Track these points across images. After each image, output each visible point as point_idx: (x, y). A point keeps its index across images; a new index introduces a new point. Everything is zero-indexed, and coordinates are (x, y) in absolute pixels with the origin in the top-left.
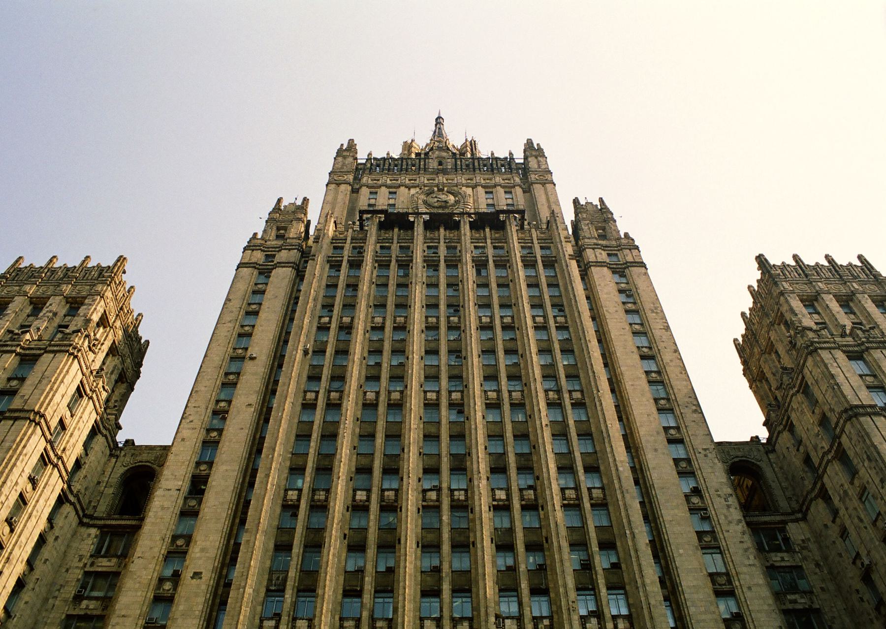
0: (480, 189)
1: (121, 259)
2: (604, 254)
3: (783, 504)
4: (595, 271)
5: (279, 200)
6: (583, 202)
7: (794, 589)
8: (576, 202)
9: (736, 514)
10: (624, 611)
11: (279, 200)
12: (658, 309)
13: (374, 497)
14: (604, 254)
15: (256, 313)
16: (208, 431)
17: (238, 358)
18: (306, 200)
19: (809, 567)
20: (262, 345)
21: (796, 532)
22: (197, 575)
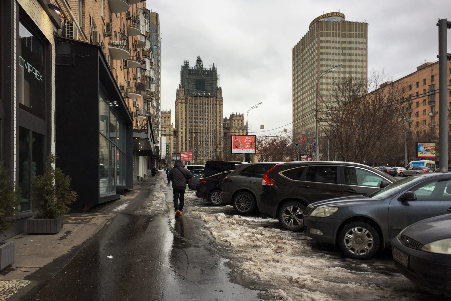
12: (222, 113)
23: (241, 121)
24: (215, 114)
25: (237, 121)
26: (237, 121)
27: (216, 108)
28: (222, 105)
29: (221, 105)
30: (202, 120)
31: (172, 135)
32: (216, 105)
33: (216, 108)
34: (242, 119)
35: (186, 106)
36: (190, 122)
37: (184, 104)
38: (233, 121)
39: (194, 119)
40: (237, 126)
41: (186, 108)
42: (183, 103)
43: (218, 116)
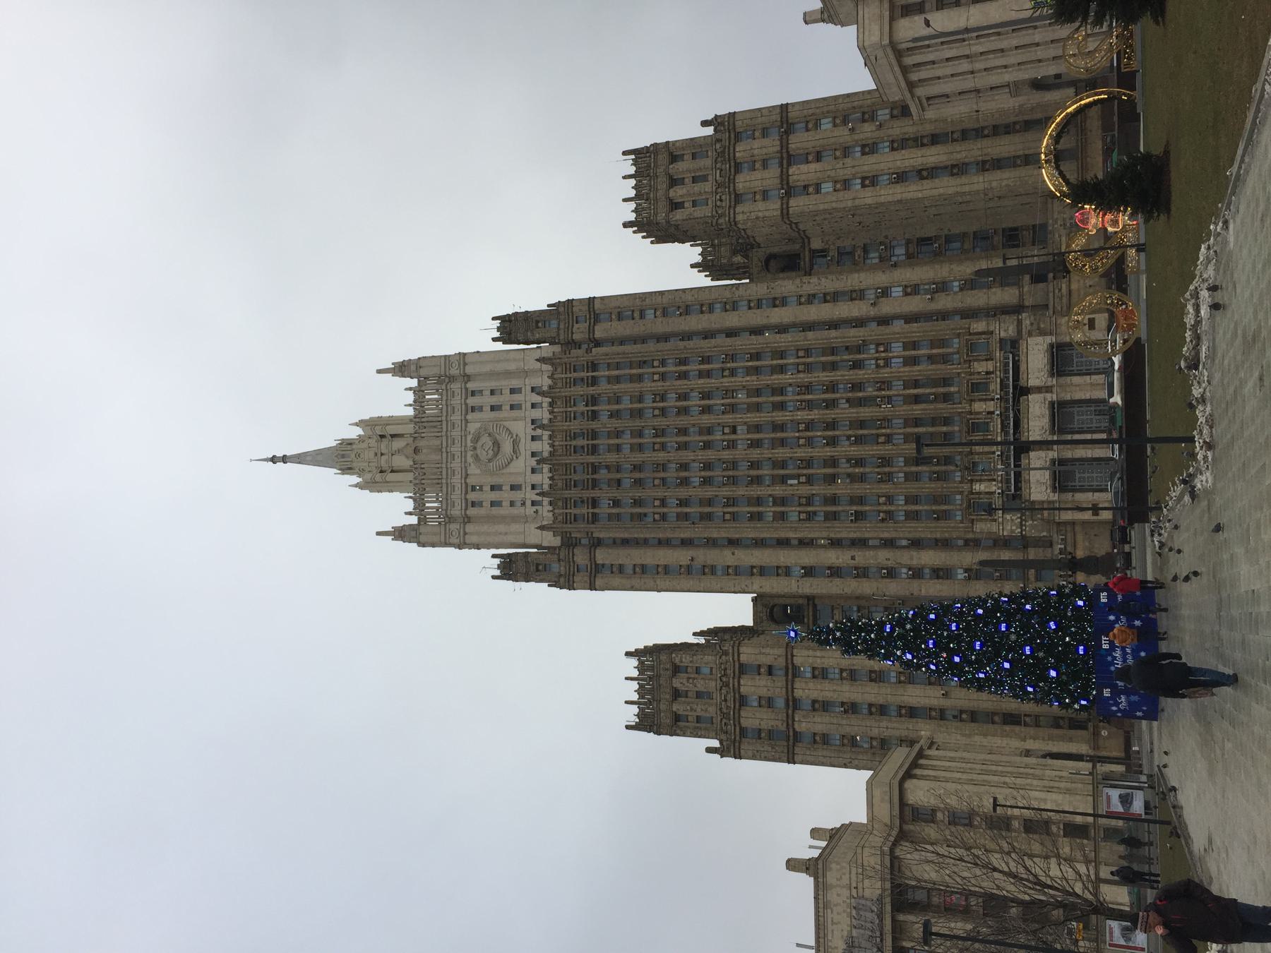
0: (469, 417)
1: (628, 654)
2: (576, 326)
3: (797, 246)
4: (598, 335)
5: (494, 577)
6: (497, 335)
7: (851, 254)
8: (494, 340)
9: (814, 280)
10: (873, 346)
11: (494, 577)
13: (805, 472)
14: (576, 326)
15: (643, 567)
16: (752, 574)
17: (688, 570)
18: (494, 556)
19: (839, 243)
20: (680, 557)
21: (816, 244)
22: (853, 558)
23: (674, 158)
24: (651, 346)
25: (678, 193)
26: (678, 193)
27: (612, 341)
28: (591, 300)
29: (592, 309)
30: (693, 438)
31: (789, 657)
32: (598, 343)
33: (612, 341)
34: (663, 158)
35: (615, 543)
36: (707, 517)
37: (602, 556)
38: (679, 215)
39: (683, 493)
40: (708, 187)
41: (625, 542)
42: (592, 559)
43: (661, 326)
